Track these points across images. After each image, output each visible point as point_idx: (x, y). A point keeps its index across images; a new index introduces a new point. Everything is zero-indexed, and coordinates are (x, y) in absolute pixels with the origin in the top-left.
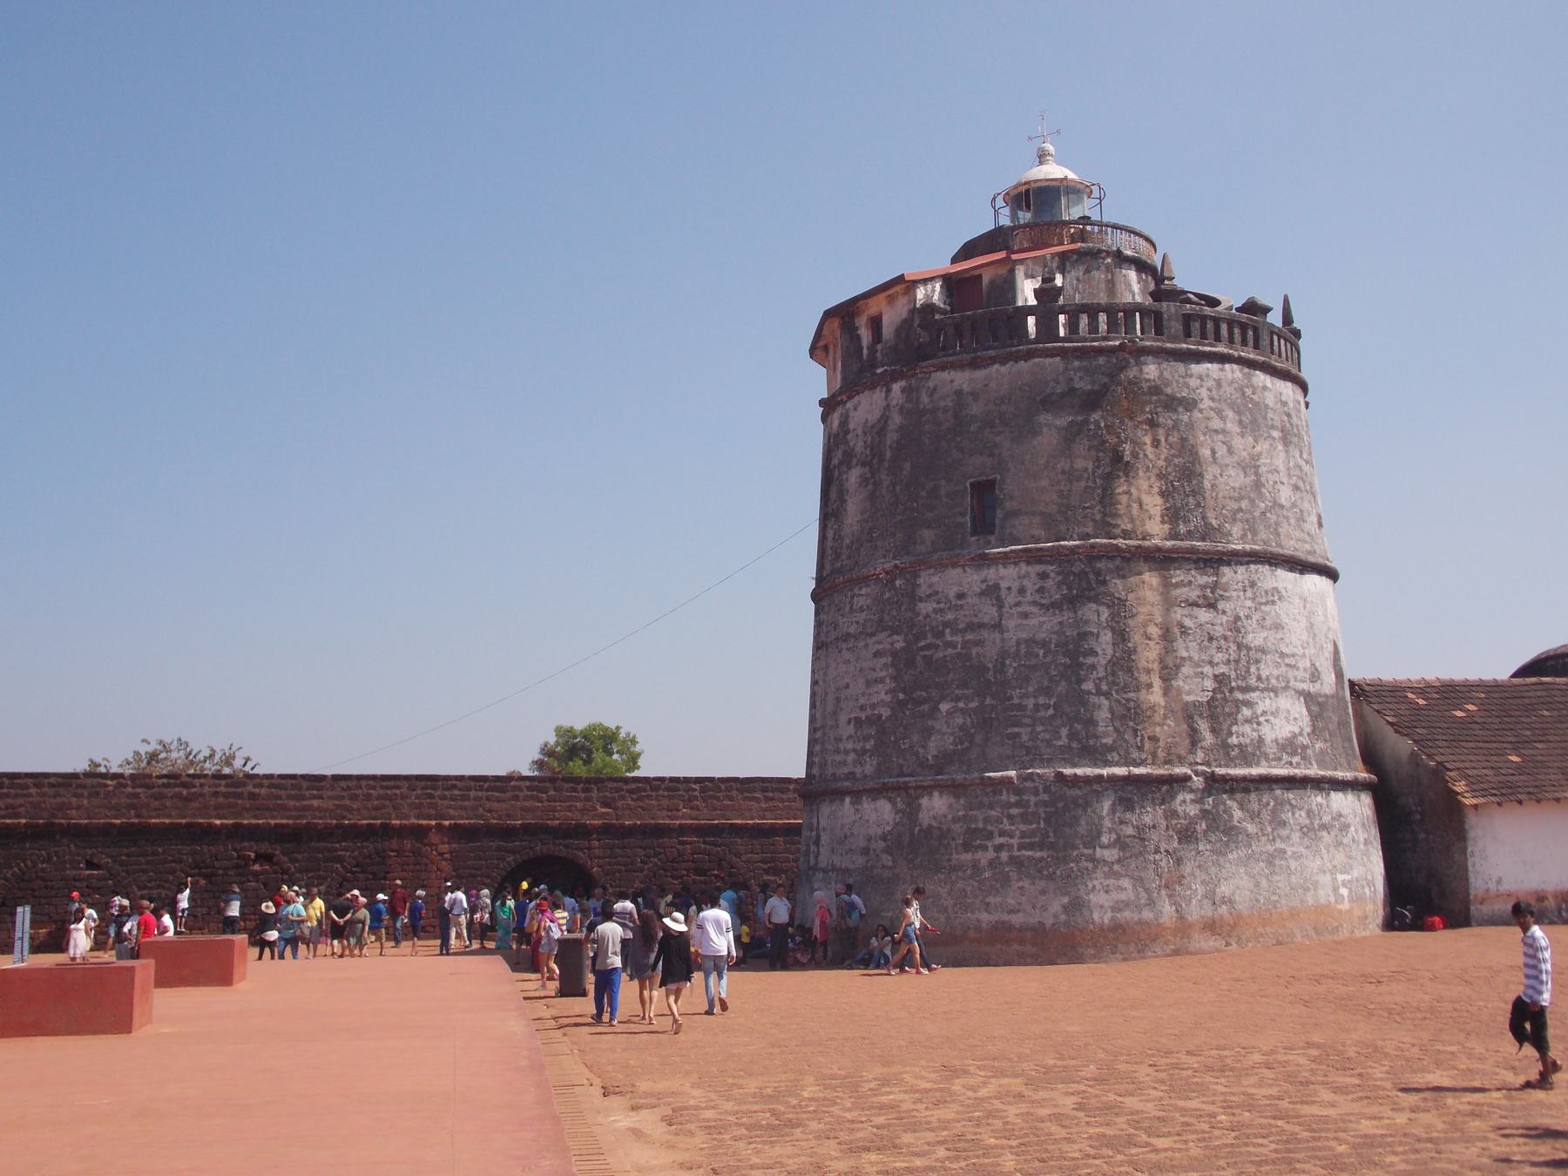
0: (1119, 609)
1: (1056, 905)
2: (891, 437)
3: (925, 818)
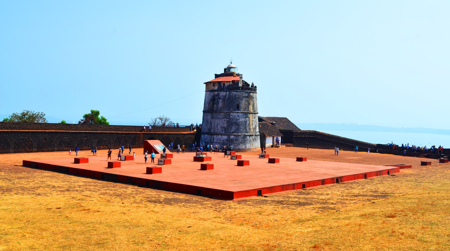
0: (249, 118)
1: (244, 147)
2: (227, 98)
3: (231, 138)
